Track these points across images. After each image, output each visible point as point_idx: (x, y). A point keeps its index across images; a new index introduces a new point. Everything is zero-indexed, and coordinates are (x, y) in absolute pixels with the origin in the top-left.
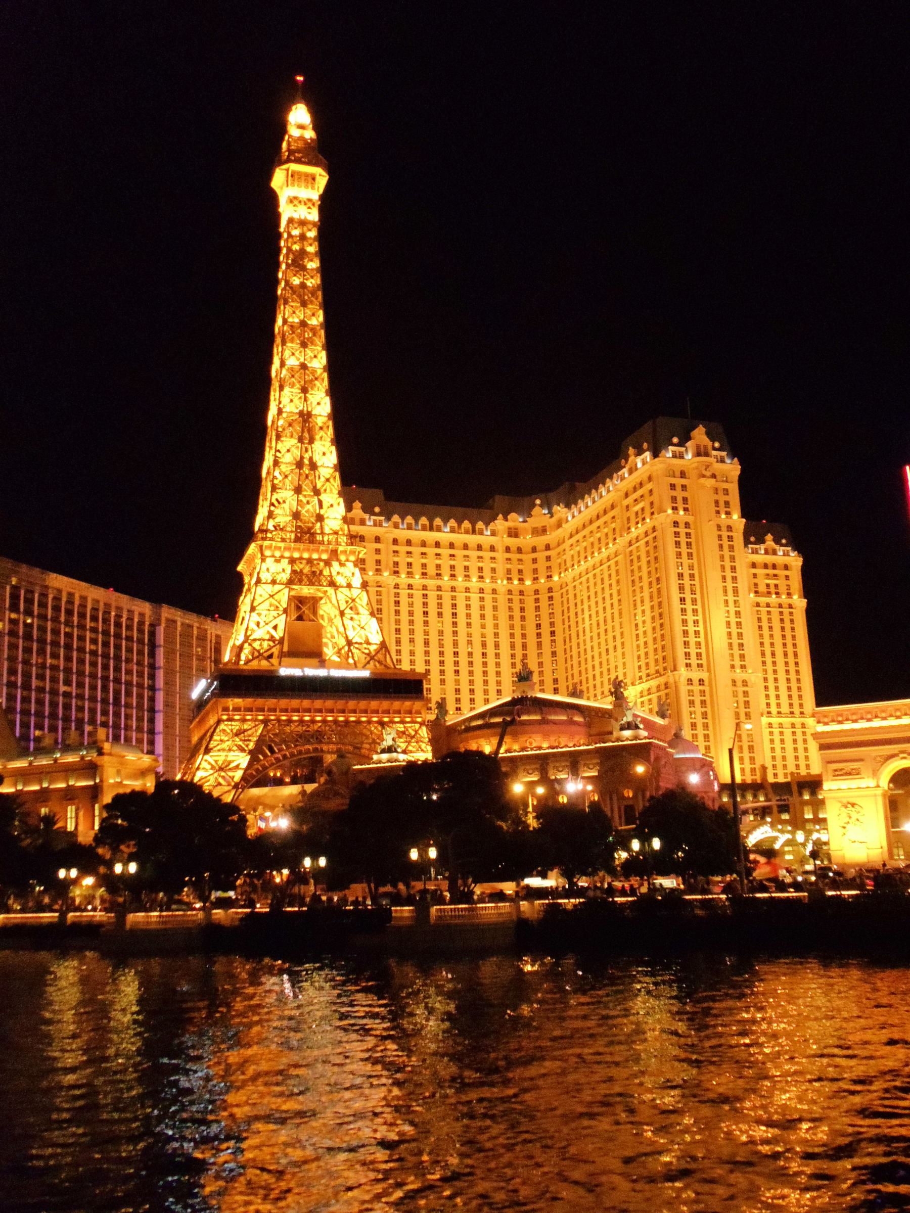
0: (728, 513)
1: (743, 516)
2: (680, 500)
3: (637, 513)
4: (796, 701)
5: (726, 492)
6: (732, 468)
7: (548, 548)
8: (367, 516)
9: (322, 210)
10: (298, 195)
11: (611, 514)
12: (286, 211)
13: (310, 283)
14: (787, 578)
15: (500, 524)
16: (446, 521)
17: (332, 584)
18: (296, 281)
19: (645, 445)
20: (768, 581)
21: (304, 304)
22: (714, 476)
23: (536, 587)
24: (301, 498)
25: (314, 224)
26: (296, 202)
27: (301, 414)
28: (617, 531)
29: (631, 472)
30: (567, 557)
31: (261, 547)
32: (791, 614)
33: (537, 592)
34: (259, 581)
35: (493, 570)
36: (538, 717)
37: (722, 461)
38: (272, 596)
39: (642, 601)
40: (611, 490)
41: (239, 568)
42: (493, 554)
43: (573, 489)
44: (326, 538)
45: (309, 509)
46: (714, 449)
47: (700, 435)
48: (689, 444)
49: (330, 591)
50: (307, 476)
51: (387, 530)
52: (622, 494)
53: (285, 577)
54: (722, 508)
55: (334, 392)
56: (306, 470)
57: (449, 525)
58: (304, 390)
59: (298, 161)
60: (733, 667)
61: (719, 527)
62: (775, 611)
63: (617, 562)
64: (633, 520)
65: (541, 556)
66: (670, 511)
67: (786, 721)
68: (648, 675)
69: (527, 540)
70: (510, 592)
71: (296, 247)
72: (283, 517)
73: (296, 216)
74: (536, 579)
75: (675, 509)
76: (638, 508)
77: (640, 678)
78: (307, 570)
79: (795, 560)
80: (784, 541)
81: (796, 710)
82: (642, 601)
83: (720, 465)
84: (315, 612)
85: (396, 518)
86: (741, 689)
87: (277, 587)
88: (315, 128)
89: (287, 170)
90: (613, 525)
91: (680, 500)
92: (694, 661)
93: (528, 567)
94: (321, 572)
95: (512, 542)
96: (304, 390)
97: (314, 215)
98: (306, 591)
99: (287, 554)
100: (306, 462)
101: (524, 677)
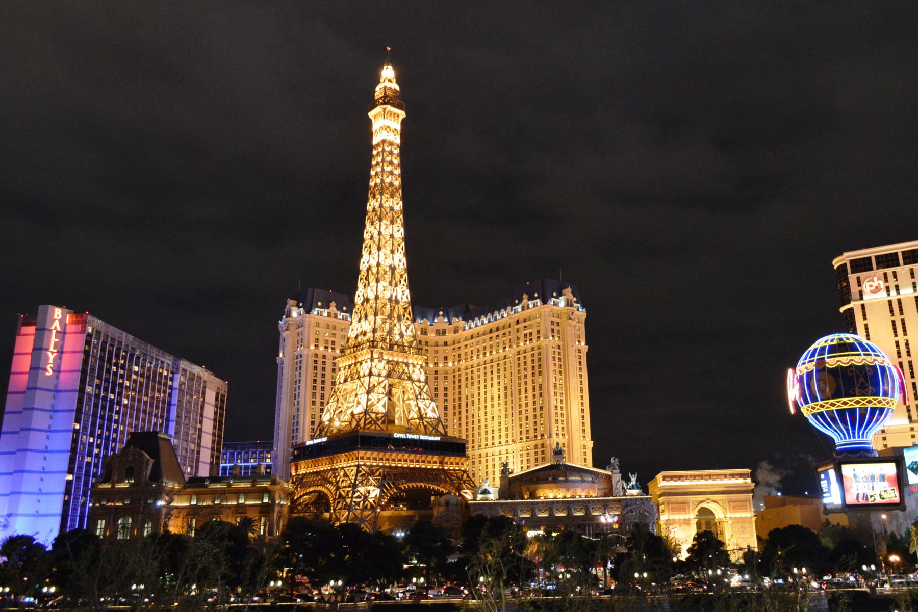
0: (579, 342)
1: (587, 344)
2: (556, 331)
3: (526, 335)
7: (446, 344)
11: (503, 331)
17: (410, 378)
23: (436, 369)
27: (390, 267)
29: (523, 309)
31: (372, 352)
33: (436, 372)
36: (578, 478)
39: (526, 391)
47: (568, 291)
52: (514, 321)
55: (408, 254)
59: (393, 105)
64: (522, 337)
65: (441, 349)
68: (527, 438)
71: (389, 159)
74: (436, 364)
75: (553, 336)
82: (526, 391)
83: (576, 312)
87: (381, 379)
88: (397, 82)
89: (384, 109)
92: (560, 432)
93: (431, 354)
96: (392, 252)
97: (397, 140)
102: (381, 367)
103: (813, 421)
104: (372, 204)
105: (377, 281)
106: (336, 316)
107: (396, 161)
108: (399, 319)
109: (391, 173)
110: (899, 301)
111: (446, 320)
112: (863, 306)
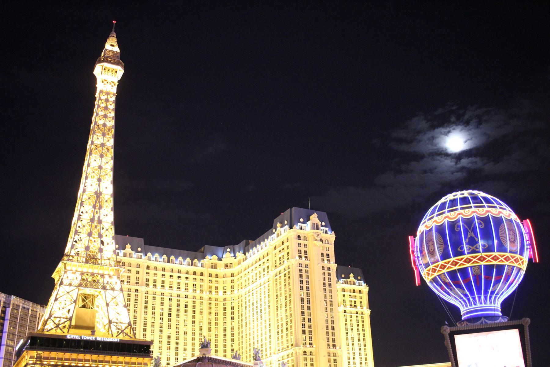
0: (328, 260)
2: (303, 252)
3: (280, 258)
6: (331, 236)
8: (133, 253)
10: (108, 77)
12: (100, 86)
14: (361, 298)
16: (177, 258)
18: (101, 122)
19: (286, 222)
20: (351, 299)
21: (104, 135)
22: (321, 240)
24: (91, 238)
25: (114, 95)
26: (105, 82)
27: (96, 193)
28: (270, 268)
30: (243, 281)
32: (362, 317)
37: (326, 232)
38: (68, 293)
41: (53, 276)
42: (202, 277)
43: (247, 244)
44: (103, 262)
45: (95, 247)
46: (322, 226)
47: (314, 218)
48: (309, 223)
49: (103, 291)
50: (96, 227)
51: (144, 261)
53: (77, 282)
54: (325, 258)
56: (96, 223)
57: (178, 260)
58: (99, 180)
59: (110, 62)
60: (329, 345)
61: (323, 268)
62: (354, 316)
63: (269, 285)
66: (297, 258)
68: (283, 349)
70: (210, 299)
72: (80, 248)
73: (104, 90)
75: (300, 257)
76: (281, 255)
77: (279, 350)
78: (90, 279)
79: (365, 289)
80: (359, 278)
83: (325, 235)
84: (93, 303)
85: (149, 254)
86: (332, 358)
87: (72, 288)
90: (268, 264)
91: (303, 252)
94: (98, 280)
96: (99, 180)
97: (114, 90)
98: (88, 291)
99: (80, 269)
100: (96, 219)
101: (205, 346)
106: (131, 256)
109: (105, 116)
111: (233, 255)
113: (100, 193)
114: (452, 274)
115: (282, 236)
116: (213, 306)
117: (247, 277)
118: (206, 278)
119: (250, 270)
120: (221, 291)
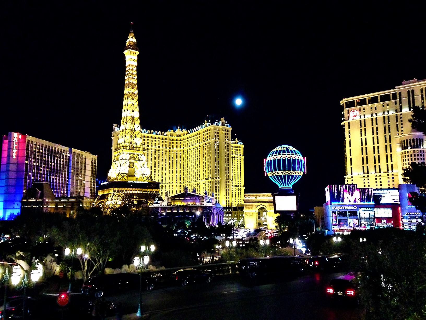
4: (239, 182)
5: (228, 134)
6: (230, 129)
9: (138, 62)
13: (134, 82)
15: (169, 132)
22: (225, 131)
34: (122, 159)
35: (166, 145)
40: (200, 130)
47: (223, 119)
55: (140, 111)
59: (133, 49)
62: (236, 159)
65: (179, 142)
67: (237, 188)
69: (175, 137)
70: (170, 151)
79: (242, 146)
81: (239, 185)
95: (171, 138)
97: (136, 64)
101: (186, 188)
102: (128, 157)
103: (271, 178)
104: (126, 91)
105: (126, 123)
107: (135, 73)
108: (136, 137)
110: (365, 120)
112: (349, 123)
113: (134, 117)
114: (277, 176)
115: (207, 127)
116: (171, 155)
117: (188, 142)
118: (168, 141)
119: (190, 139)
120: (175, 147)
